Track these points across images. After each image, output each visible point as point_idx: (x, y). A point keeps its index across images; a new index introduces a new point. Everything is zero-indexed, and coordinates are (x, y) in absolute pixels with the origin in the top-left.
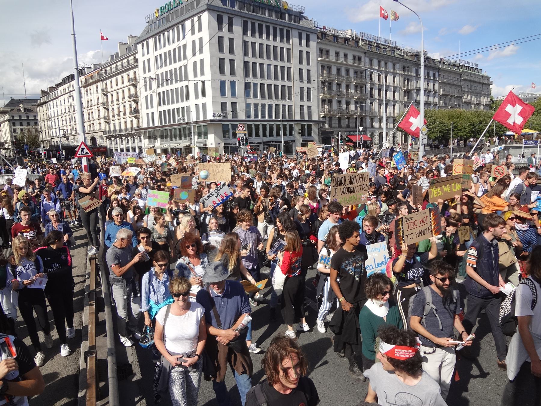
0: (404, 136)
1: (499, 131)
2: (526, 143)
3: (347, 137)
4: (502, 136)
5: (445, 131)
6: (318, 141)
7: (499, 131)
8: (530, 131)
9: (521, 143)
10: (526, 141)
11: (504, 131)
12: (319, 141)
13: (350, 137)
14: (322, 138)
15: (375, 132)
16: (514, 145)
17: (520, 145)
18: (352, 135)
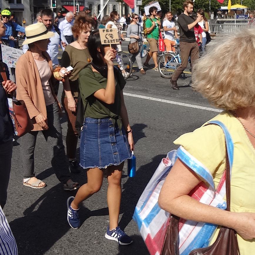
0: (124, 8)
1: (215, 6)
2: (237, 17)
3: (63, 7)
4: (218, 11)
5: (164, 2)
6: (29, 10)
7: (215, 6)
8: (241, 7)
9: (234, 18)
10: (238, 15)
11: (219, 7)
12: (31, 10)
13: (66, 7)
14: (34, 7)
15: (94, 4)
16: (228, 20)
17: (233, 20)
18: (68, 5)
